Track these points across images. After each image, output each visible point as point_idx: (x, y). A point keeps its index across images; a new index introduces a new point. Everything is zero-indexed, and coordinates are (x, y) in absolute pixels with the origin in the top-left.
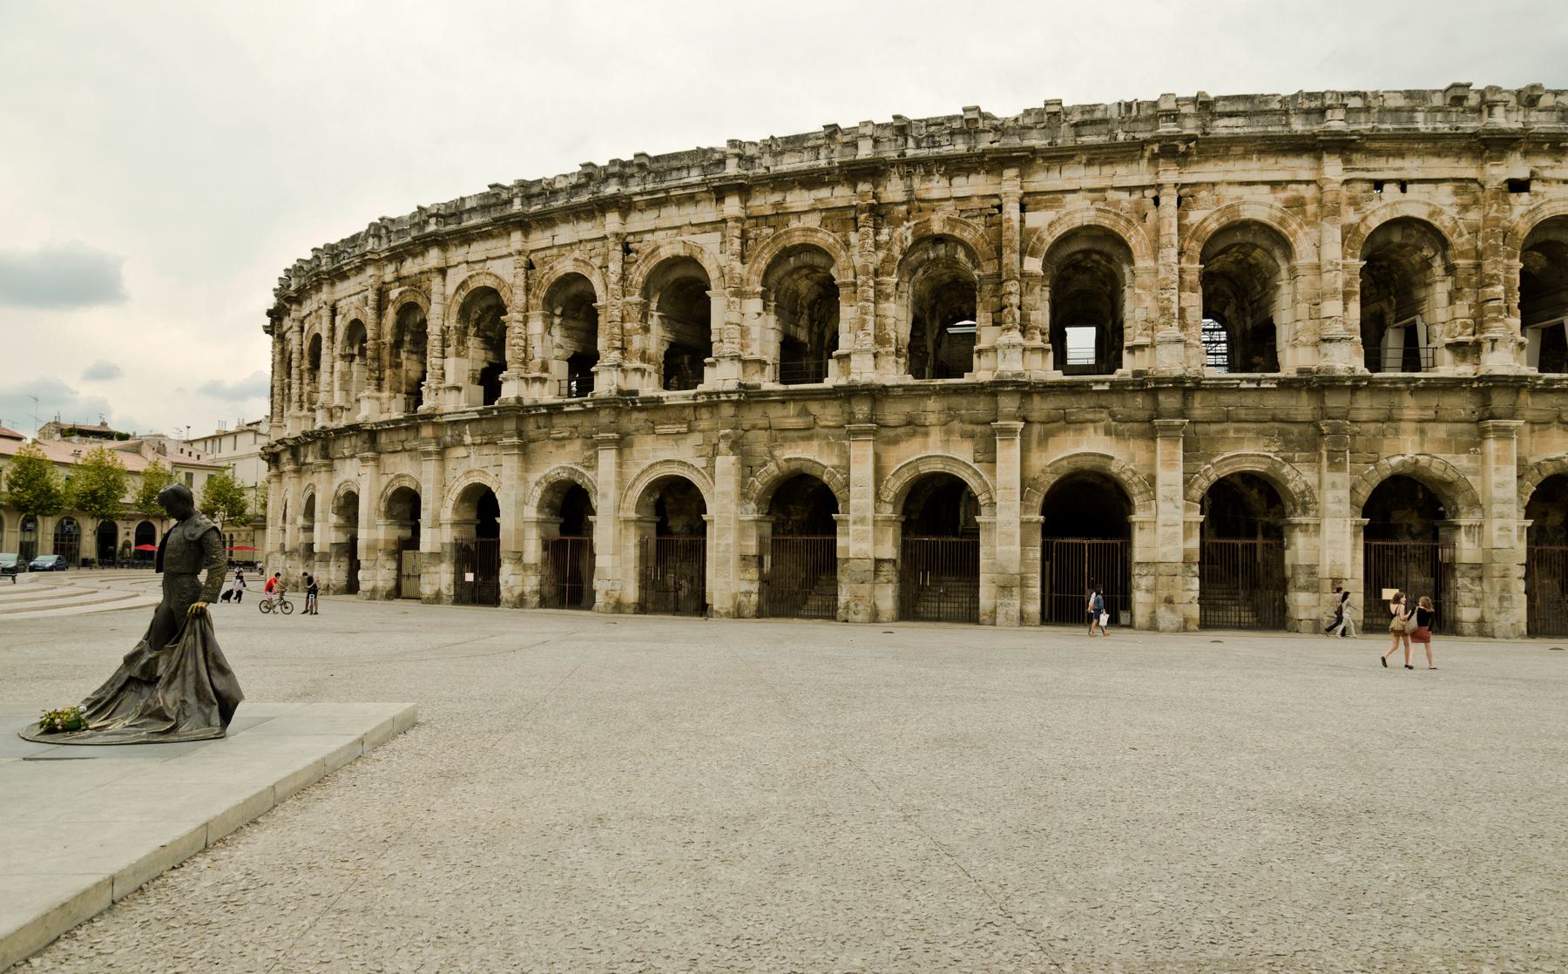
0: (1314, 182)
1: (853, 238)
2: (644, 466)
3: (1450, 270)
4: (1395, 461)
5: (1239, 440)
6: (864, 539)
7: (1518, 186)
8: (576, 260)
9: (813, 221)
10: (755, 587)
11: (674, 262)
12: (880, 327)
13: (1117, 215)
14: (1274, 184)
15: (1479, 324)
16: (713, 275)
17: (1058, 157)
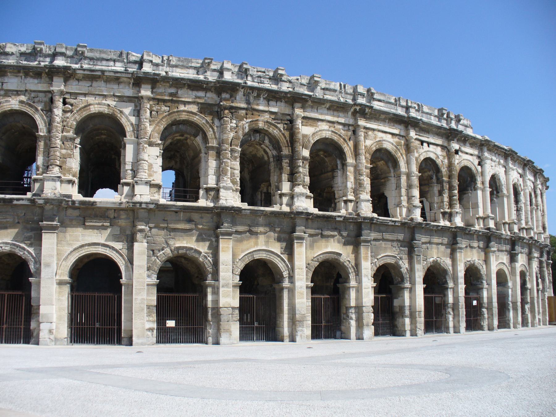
0: (405, 137)
1: (217, 122)
2: (75, 247)
3: (440, 181)
4: (431, 260)
5: (386, 249)
6: (228, 296)
7: (457, 152)
8: (21, 102)
9: (194, 108)
10: (155, 326)
11: (100, 115)
12: (233, 175)
13: (340, 136)
14: (393, 134)
15: (451, 205)
16: (129, 129)
17: (318, 103)
